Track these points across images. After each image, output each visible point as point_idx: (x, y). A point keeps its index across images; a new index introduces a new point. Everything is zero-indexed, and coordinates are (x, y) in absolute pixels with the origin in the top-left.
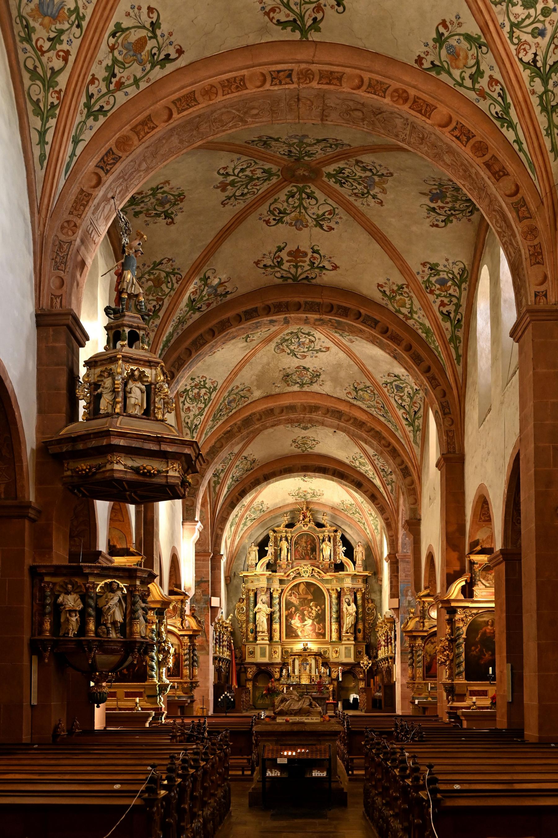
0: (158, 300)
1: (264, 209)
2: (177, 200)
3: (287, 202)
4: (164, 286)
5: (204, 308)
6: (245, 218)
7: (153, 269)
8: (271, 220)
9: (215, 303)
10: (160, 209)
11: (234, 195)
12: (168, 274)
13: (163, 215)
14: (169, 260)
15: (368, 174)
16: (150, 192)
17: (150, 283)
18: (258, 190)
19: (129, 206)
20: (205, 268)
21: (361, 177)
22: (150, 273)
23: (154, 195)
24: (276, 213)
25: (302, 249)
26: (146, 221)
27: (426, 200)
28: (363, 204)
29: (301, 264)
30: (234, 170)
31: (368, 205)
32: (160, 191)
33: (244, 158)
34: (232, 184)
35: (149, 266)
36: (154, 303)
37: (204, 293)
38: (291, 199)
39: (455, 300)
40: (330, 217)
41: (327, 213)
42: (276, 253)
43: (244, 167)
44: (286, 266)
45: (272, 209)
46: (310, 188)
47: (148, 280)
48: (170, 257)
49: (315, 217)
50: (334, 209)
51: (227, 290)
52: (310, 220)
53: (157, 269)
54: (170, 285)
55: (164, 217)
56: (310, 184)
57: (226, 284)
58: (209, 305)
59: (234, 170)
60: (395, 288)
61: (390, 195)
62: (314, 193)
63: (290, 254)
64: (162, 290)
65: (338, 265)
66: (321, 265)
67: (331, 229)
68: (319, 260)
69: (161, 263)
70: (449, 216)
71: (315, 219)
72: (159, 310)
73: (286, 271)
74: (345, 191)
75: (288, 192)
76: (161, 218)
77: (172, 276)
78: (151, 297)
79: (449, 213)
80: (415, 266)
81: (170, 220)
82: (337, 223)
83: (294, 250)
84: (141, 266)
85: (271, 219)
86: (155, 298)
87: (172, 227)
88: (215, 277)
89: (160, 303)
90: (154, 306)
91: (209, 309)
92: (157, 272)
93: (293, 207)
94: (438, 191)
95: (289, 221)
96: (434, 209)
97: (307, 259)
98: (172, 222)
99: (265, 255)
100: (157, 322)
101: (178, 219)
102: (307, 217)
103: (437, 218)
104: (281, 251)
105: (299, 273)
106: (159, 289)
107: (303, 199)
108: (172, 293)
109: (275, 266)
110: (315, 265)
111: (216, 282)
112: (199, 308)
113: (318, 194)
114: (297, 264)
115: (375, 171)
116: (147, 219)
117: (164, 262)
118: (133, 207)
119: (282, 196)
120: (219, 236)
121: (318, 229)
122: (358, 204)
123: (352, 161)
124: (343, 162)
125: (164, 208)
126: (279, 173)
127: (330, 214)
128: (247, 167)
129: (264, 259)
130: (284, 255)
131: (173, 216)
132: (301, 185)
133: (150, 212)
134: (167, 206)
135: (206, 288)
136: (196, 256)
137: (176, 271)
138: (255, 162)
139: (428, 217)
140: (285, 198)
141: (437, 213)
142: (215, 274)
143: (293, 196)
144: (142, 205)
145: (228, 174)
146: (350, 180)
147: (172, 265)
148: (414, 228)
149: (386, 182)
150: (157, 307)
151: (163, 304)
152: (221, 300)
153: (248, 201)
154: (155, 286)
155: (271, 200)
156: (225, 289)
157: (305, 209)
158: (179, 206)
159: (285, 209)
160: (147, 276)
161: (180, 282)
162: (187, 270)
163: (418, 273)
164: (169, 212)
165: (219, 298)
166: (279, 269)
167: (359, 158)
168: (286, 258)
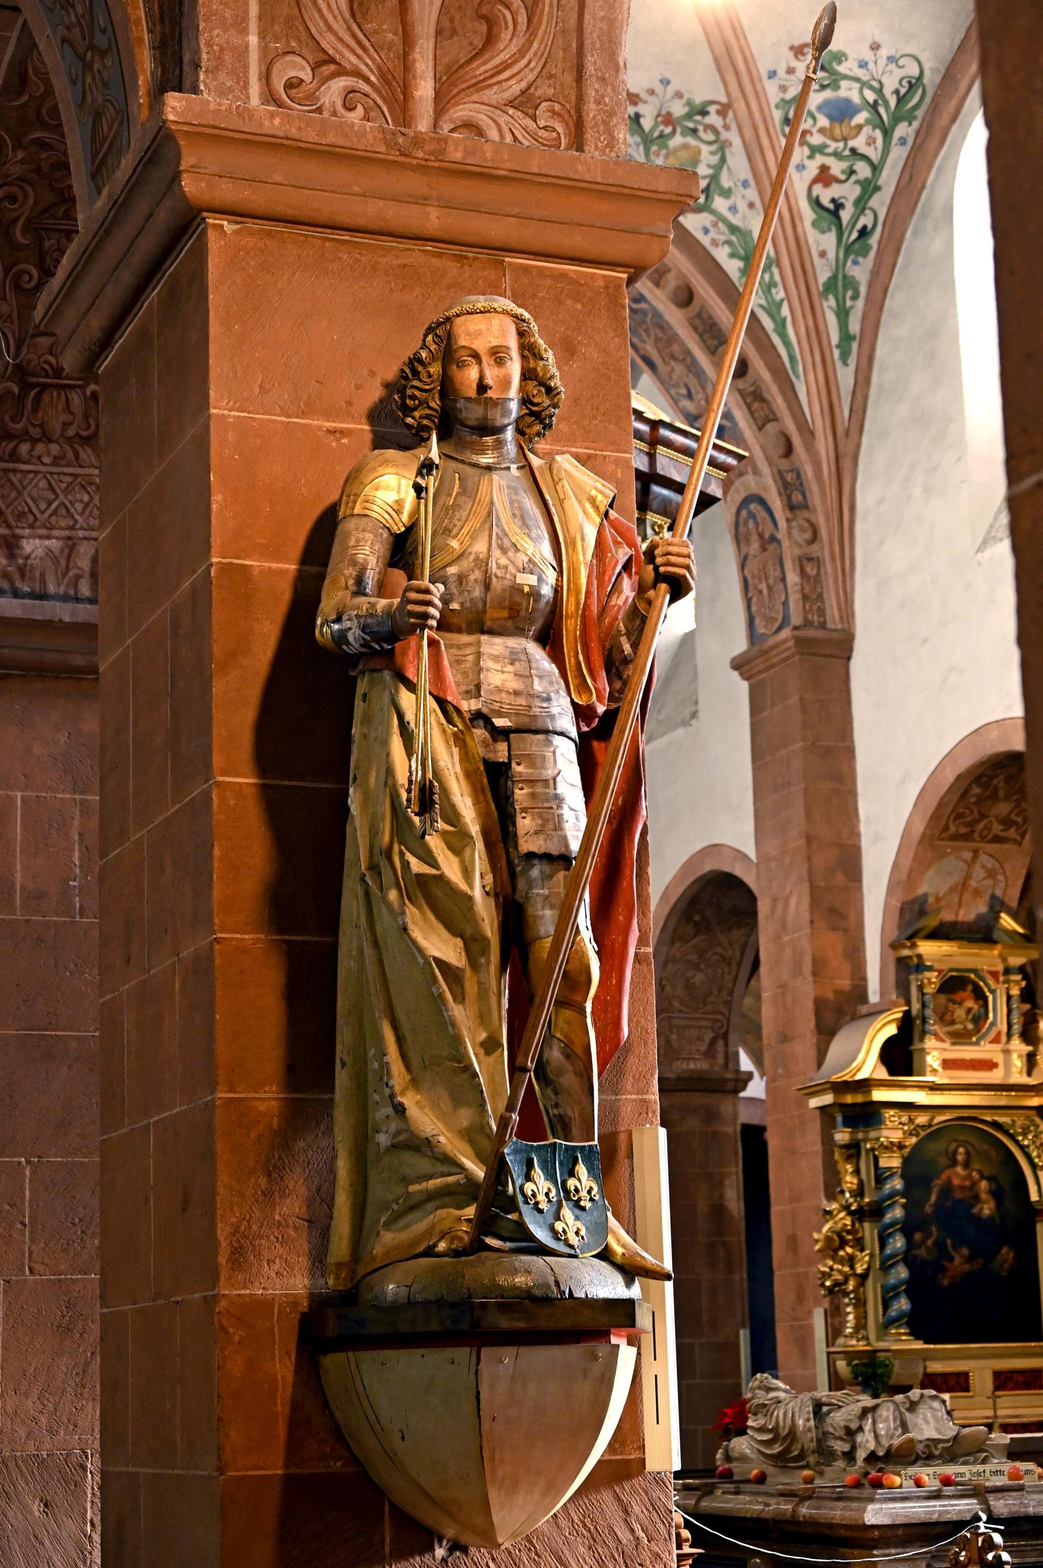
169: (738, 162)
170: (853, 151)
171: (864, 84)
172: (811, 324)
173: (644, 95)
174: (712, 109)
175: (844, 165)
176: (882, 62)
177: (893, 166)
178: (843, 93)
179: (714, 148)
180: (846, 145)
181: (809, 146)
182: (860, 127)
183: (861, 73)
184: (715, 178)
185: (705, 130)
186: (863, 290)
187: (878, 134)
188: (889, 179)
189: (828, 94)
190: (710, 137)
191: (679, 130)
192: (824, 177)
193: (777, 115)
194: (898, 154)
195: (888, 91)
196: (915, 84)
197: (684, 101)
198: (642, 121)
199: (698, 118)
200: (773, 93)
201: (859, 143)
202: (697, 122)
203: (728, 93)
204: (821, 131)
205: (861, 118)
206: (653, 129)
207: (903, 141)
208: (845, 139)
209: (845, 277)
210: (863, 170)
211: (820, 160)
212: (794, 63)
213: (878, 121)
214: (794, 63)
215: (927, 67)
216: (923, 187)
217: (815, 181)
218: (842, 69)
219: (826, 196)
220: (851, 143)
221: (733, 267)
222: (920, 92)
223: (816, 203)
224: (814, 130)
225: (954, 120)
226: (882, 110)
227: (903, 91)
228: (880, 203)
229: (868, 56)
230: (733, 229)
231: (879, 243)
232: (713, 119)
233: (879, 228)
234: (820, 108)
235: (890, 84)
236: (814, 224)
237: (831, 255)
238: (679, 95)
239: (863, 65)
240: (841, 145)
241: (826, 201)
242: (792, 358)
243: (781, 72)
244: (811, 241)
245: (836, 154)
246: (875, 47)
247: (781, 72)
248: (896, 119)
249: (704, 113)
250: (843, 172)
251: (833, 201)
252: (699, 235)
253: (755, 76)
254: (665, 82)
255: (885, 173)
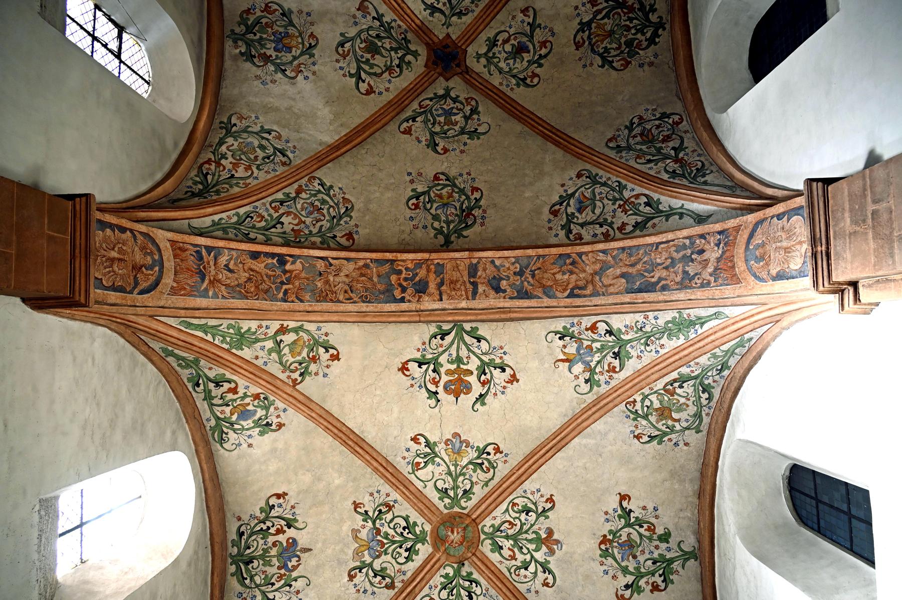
0: (673, 393)
1: (502, 470)
2: (611, 541)
3: (472, 483)
4: (657, 405)
5: (602, 327)
6: (527, 459)
7: (665, 434)
8: (492, 452)
9: (583, 326)
10: (635, 537)
11: (539, 516)
12: (645, 417)
13: (633, 520)
14: (638, 437)
15: (377, 565)
16: (642, 582)
17: (675, 415)
18: (507, 510)
19: (671, 561)
20: (590, 398)
21: (386, 554)
22: (672, 429)
23: (639, 576)
24: (486, 463)
25: (452, 398)
26: (657, 517)
27: (303, 538)
28: (378, 492)
29: (453, 367)
30: (535, 573)
31: (372, 494)
32: (630, 579)
33: (522, 588)
34: (539, 541)
35: (670, 440)
36: (679, 391)
37: (597, 357)
38: (468, 487)
39: (216, 401)
40: (418, 460)
41: (422, 465)
42: (487, 392)
43: (523, 571)
44: (473, 364)
45: (492, 470)
46: (445, 506)
47: (679, 421)
48: (636, 441)
49: (437, 460)
50: (413, 472)
51: (561, 343)
52: (443, 454)
53: (659, 430)
54: (647, 403)
55: (632, 515)
56: (446, 511)
57: (563, 357)
58: (593, 328)
59: (535, 573)
60: (313, 367)
61: (346, 528)
62: (440, 499)
63: (468, 389)
64: (661, 402)
65: (400, 373)
66: (424, 367)
67: (415, 440)
68: (428, 377)
69: (652, 438)
70: (267, 518)
71: (437, 456)
72: (675, 381)
73: (474, 353)
74: (404, 508)
75: (471, 499)
76: (636, 515)
77: (640, 412)
78: (682, 400)
79: (269, 524)
80: (294, 419)
81: (625, 504)
82: (408, 450)
83: (462, 395)
84: (681, 444)
85: (492, 454)
86: (676, 397)
87: (624, 490)
88: (577, 377)
89: (669, 387)
90: (681, 387)
91: (594, 319)
92: (660, 426)
93: (464, 474)
94: (290, 565)
95: (469, 449)
96: (289, 526)
97: (445, 378)
98: (623, 497)
99: (503, 393)
100: (685, 370)
101: (613, 503)
102: (446, 459)
103: (281, 510)
104: (481, 395)
105: (455, 346)
106: (666, 405)
107: (453, 488)
108: (646, 391)
109: (488, 365)
110: (432, 367)
111: (578, 368)
112: (610, 332)
113: (434, 496)
114: (458, 367)
115: (371, 574)
116: (653, 520)
117: (645, 439)
118: (669, 556)
119: (479, 492)
120: (563, 443)
121: (432, 439)
122: (386, 488)
123: (399, 585)
124: (409, 574)
125: (629, 534)
126: (483, 537)
127: (418, 464)
128: (519, 568)
129: (504, 384)
130: (477, 389)
131: (620, 512)
132: (456, 509)
133: (647, 534)
134: (624, 538)
135: (593, 364)
136: (599, 426)
137: (632, 416)
138: (511, 574)
139: (293, 507)
140: (476, 489)
141: (283, 519)
142: (576, 383)
143: (465, 492)
144: (656, 555)
145: (546, 569)
146: (398, 538)
147: (636, 427)
148: (307, 478)
149: (357, 553)
150: (676, 385)
151: (666, 385)
152: (573, 325)
153: (519, 491)
154: (670, 410)
155: (492, 484)
156: (565, 347)
157: (449, 473)
158: (608, 526)
159: (475, 471)
160: (678, 427)
161: (631, 399)
162: (615, 409)
163: (285, 410)
164: (622, 520)
165: (575, 329)
166: (483, 357)
167: (392, 593)
168: (472, 379)
169: (275, 369)
170: (229, 405)
171: (243, 429)
172: (195, 348)
173: (330, 362)
174: (300, 379)
175: (227, 399)
176: (242, 442)
177: (205, 411)
178: (250, 421)
179: (288, 363)
180: (233, 405)
181: (249, 396)
182: (232, 414)
183: (248, 433)
184: (279, 352)
185: (296, 367)
186: (178, 369)
187: (222, 416)
188: (203, 406)
189: (256, 418)
190: (292, 367)
191: (307, 358)
192: (234, 391)
193: (271, 398)
194: (206, 413)
195: (231, 433)
196: (222, 441)
197: (313, 373)
198: (324, 350)
199: (302, 371)
200: (280, 404)
201: (228, 410)
202: (301, 369)
203: (297, 391)
204: (249, 404)
205: (234, 418)
206: (317, 349)
207: (208, 420)
208: (235, 407)
209: (191, 367)
210: (216, 401)
211: (241, 394)
212: (279, 420)
213: (226, 420)
214: (279, 420)
215: (222, 451)
216: (187, 422)
217: (236, 387)
218: (258, 430)
219: (226, 386)
220: (231, 407)
221: (245, 325)
222: (217, 439)
223: (229, 382)
224: (251, 403)
225: (197, 451)
226: (227, 425)
227: (224, 435)
228: (199, 398)
229: (250, 441)
230: (257, 340)
231: (186, 386)
232: (296, 375)
233: (191, 389)
234: (256, 411)
235: (232, 435)
236: (225, 375)
237: (206, 371)
238: (316, 374)
239: (250, 436)
240: (235, 405)
241: (225, 384)
242: (189, 325)
243: (282, 414)
244: (220, 369)
245: (235, 400)
246: (250, 446)
247: (282, 414)
248: (217, 425)
249: (302, 374)
250: (226, 396)
251: (222, 386)
252: (268, 323)
253: (291, 405)
254: (325, 375)
255: (206, 406)
